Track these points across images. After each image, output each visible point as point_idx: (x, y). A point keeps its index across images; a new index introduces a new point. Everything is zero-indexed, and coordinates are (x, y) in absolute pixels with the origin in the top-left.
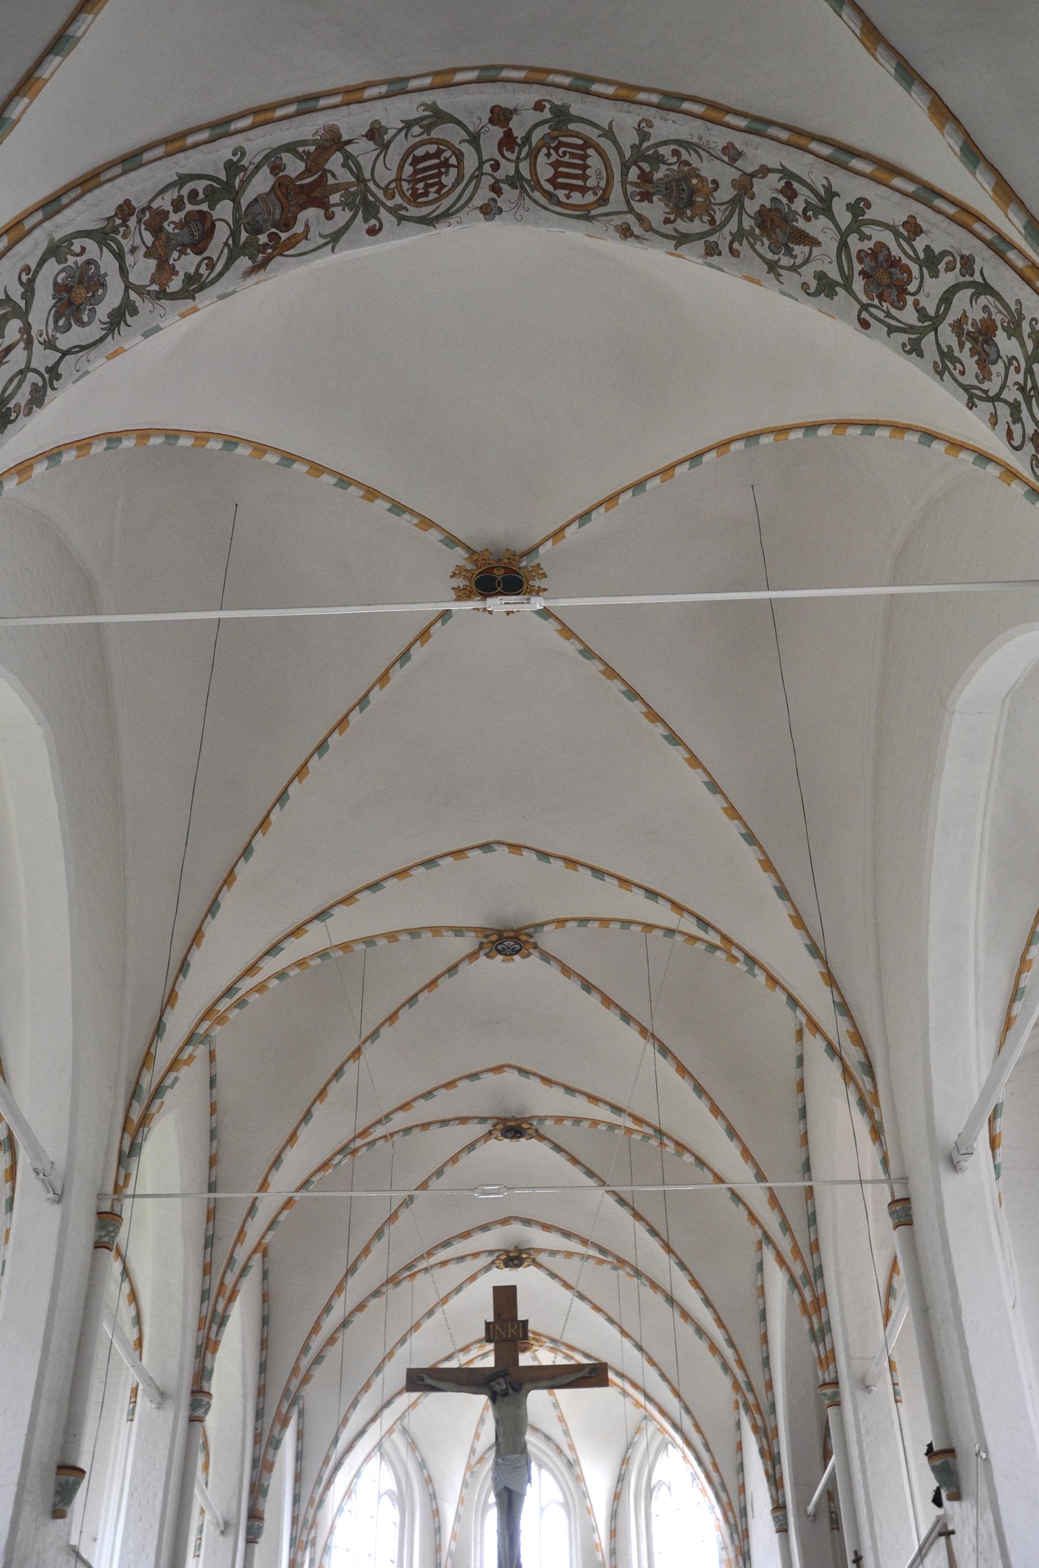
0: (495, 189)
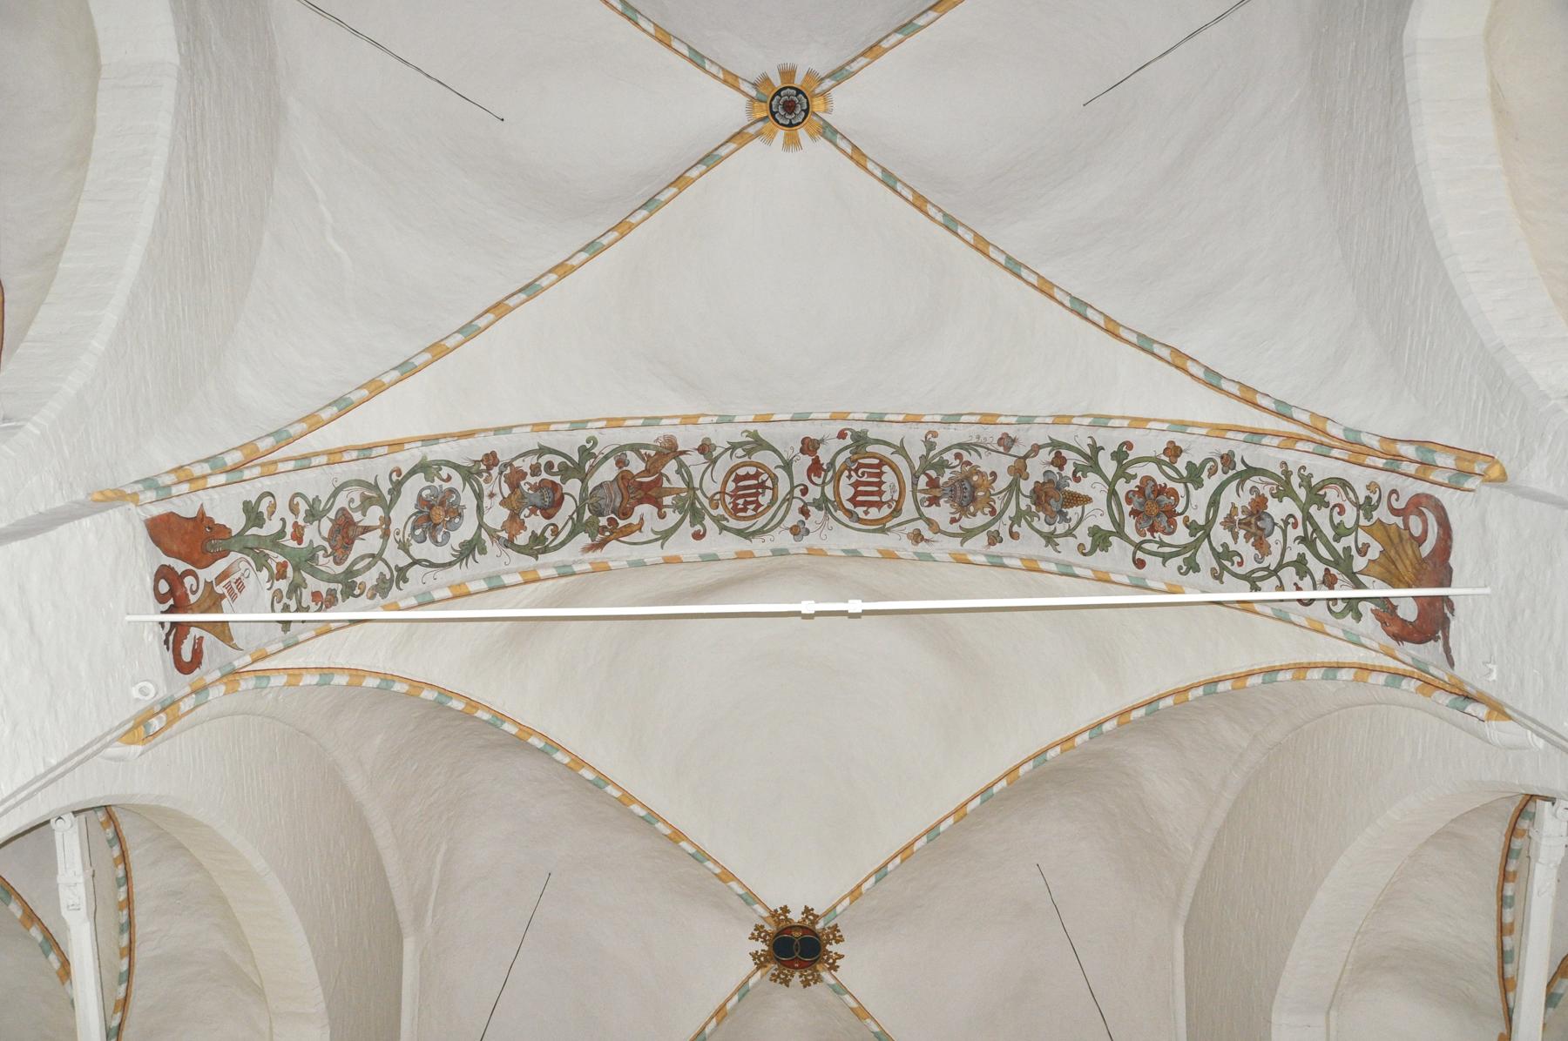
0: (804, 512)
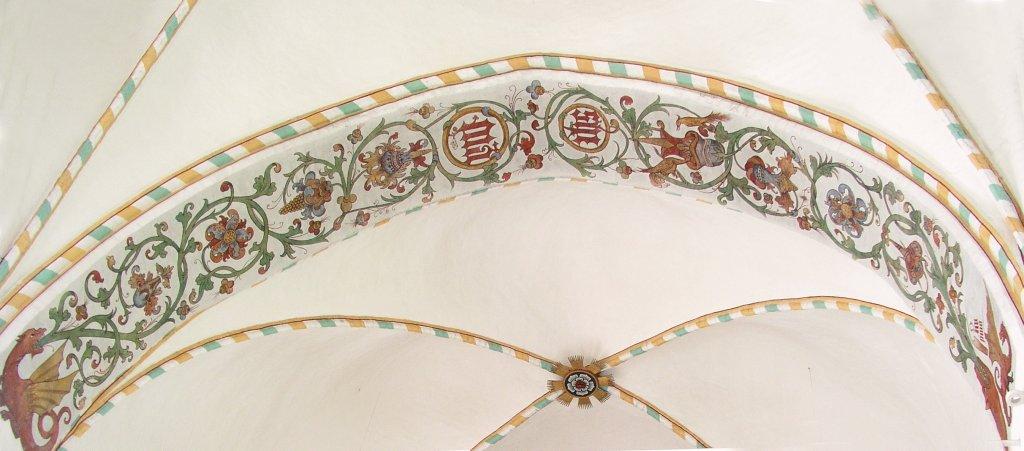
0: (533, 107)
